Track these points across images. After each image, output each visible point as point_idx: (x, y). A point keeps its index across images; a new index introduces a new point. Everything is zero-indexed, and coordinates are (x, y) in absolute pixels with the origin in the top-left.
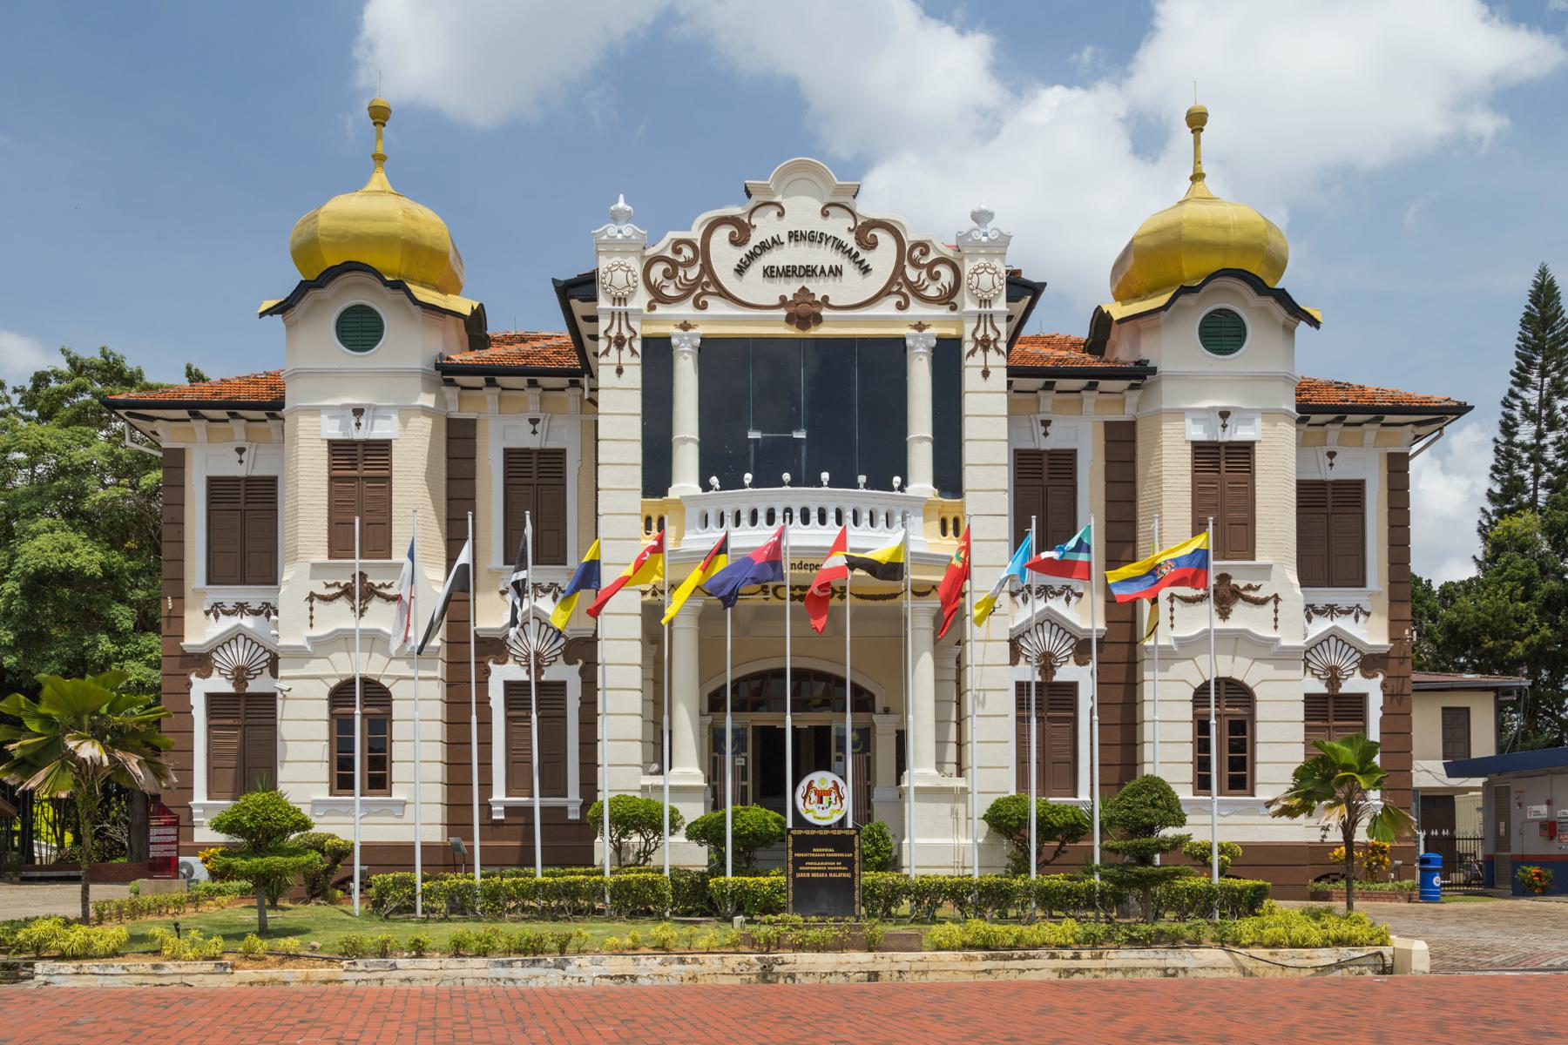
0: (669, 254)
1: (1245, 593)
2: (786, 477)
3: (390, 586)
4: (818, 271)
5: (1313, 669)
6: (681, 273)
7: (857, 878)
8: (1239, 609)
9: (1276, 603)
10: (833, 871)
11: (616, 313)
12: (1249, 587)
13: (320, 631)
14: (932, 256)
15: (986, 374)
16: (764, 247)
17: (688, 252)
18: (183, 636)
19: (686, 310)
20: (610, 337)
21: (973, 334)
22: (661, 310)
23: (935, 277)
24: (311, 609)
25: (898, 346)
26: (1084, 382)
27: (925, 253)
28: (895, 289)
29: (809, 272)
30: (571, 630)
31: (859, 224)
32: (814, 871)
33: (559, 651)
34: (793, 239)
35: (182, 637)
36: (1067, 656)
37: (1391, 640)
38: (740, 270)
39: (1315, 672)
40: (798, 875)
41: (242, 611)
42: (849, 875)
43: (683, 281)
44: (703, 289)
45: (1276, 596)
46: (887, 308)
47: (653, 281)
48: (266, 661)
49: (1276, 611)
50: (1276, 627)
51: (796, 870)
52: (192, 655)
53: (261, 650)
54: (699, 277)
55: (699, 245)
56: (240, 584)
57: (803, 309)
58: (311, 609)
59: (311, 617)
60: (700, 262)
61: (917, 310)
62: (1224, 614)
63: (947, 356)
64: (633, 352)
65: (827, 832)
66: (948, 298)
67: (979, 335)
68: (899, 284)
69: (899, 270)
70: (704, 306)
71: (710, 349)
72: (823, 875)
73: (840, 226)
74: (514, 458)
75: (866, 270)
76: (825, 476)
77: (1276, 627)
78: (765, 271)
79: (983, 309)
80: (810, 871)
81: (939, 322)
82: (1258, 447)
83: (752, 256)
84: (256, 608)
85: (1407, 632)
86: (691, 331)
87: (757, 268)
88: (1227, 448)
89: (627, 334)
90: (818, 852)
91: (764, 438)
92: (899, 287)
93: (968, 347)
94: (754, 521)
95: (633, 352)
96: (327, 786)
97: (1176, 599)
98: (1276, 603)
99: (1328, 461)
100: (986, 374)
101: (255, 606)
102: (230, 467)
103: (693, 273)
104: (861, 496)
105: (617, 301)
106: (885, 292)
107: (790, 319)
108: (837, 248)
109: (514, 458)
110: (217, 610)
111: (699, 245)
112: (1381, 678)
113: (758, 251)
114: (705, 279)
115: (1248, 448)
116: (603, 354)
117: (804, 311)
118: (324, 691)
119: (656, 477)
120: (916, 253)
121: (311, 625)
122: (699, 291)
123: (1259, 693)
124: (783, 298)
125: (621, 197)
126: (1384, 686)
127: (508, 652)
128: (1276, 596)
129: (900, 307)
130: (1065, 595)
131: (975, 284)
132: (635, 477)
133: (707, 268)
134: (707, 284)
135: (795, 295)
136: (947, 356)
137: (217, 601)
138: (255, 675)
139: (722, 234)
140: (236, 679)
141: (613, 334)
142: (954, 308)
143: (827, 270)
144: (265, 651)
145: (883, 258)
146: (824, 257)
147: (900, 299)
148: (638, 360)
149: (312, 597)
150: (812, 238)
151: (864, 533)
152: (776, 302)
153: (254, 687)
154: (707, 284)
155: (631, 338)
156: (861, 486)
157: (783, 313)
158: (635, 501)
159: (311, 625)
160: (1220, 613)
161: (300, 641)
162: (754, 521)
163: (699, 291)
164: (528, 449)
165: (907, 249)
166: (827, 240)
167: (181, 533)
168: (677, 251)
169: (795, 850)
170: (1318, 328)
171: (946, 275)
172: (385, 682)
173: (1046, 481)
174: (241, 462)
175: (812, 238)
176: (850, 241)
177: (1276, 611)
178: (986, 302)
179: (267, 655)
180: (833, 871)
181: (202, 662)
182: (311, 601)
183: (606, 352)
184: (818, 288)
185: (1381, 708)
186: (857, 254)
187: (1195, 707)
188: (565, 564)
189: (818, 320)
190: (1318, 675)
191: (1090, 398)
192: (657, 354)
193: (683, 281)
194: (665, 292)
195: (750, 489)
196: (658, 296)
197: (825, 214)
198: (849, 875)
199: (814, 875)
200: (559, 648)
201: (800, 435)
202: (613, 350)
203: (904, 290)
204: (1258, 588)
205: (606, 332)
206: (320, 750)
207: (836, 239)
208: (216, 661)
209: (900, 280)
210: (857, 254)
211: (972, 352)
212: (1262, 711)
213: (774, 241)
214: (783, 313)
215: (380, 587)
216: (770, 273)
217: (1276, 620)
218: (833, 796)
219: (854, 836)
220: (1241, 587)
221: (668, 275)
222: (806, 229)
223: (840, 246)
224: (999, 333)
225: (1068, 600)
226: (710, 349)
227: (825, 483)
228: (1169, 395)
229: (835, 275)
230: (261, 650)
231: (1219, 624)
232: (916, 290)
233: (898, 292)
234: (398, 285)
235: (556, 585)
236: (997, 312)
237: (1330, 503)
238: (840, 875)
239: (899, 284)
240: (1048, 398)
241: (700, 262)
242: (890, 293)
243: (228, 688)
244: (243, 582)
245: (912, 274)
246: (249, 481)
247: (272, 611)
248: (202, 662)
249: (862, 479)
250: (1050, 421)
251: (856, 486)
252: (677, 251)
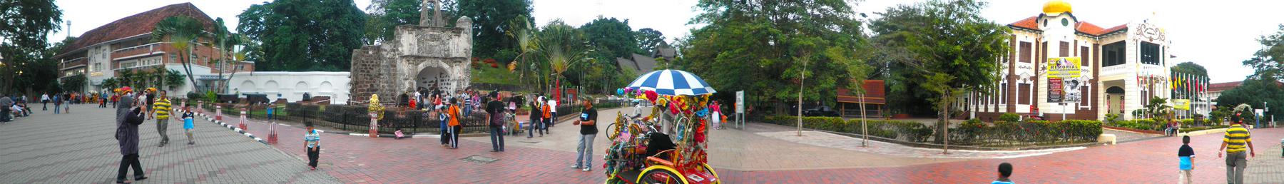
25: (1159, 45)
61: (1162, 42)
74: (1082, 47)
102: (1024, 40)
109: (1082, 47)
181: (1018, 77)
184: (1153, 36)
243: (1023, 82)
248: (1018, 77)
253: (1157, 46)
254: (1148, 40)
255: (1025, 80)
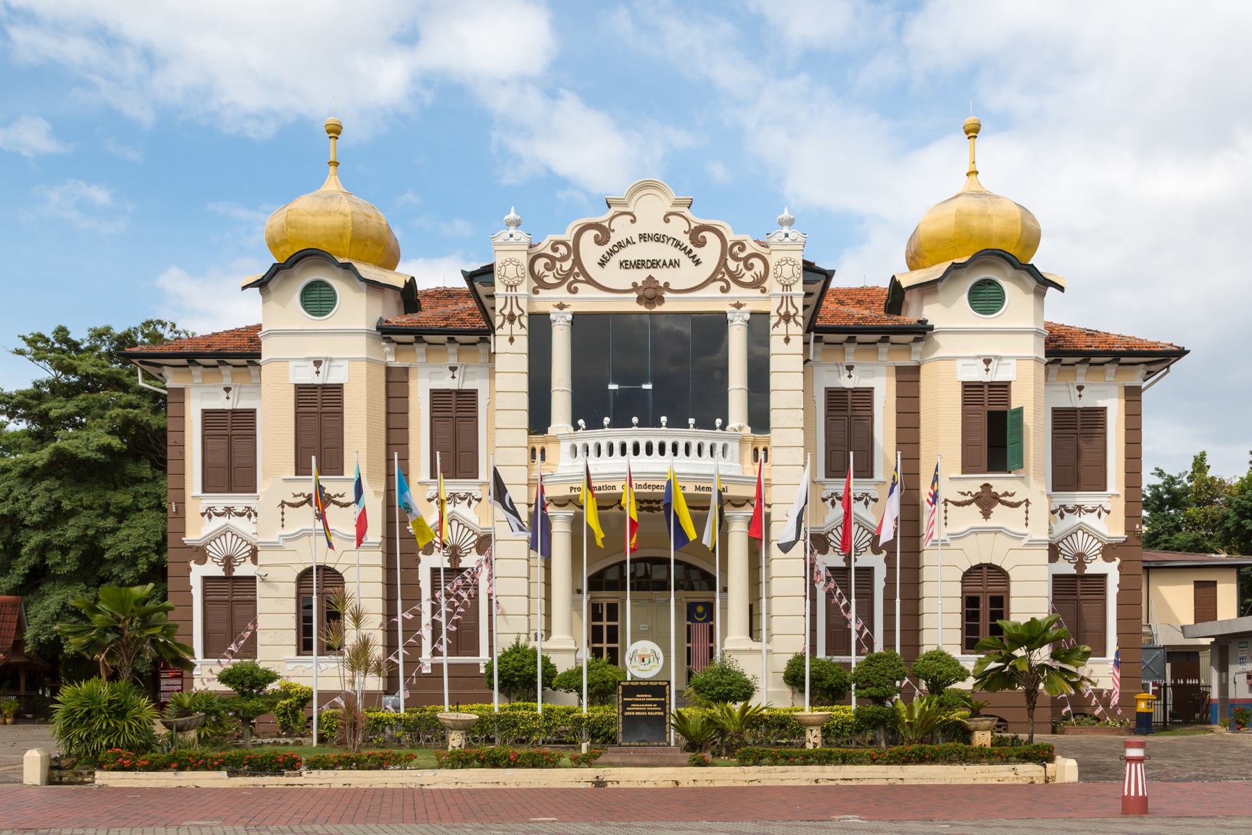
0: (549, 251)
1: (1003, 498)
2: (635, 420)
3: (342, 496)
4: (661, 264)
5: (1064, 555)
6: (558, 265)
7: (621, 712)
8: (998, 509)
9: (1027, 506)
10: (651, 711)
11: (509, 297)
12: (1006, 494)
13: (289, 530)
14: (748, 251)
15: (787, 340)
16: (620, 245)
17: (563, 250)
18: (184, 533)
19: (561, 293)
20: (504, 315)
21: (778, 311)
22: (543, 293)
23: (749, 267)
24: (283, 513)
26: (878, 337)
27: (743, 249)
28: (720, 276)
29: (654, 264)
30: (482, 529)
31: (692, 227)
32: (636, 710)
33: (473, 545)
34: (642, 240)
35: (183, 533)
36: (866, 547)
37: (1127, 532)
38: (602, 264)
39: (1066, 557)
40: (626, 714)
41: (230, 513)
42: (662, 714)
43: (560, 272)
44: (574, 278)
45: (1027, 501)
46: (714, 290)
47: (536, 272)
48: (248, 551)
49: (1027, 512)
50: (1027, 525)
51: (624, 710)
52: (191, 547)
53: (245, 543)
54: (572, 269)
55: (571, 244)
56: (228, 492)
57: (650, 293)
58: (283, 513)
59: (283, 520)
60: (572, 257)
61: (736, 291)
62: (986, 514)
63: (758, 326)
64: (522, 326)
65: (646, 683)
66: (758, 284)
67: (782, 311)
68: (723, 273)
69: (723, 263)
70: (575, 291)
71: (580, 322)
72: (643, 713)
73: (678, 229)
74: (437, 396)
75: (697, 263)
76: (664, 419)
77: (1027, 525)
78: (621, 264)
79: (785, 292)
80: (635, 711)
81: (754, 301)
82: (1012, 384)
83: (612, 253)
84: (241, 511)
85: (1137, 526)
86: (565, 310)
87: (616, 260)
88: (990, 386)
89: (517, 312)
90: (640, 697)
91: (620, 389)
92: (723, 275)
93: (773, 320)
94: (611, 453)
95: (522, 326)
96: (294, 649)
97: (948, 503)
98: (1027, 506)
99: (1078, 393)
100: (787, 340)
101: (240, 510)
103: (567, 265)
104: (690, 435)
105: (509, 288)
106: (712, 279)
107: (639, 300)
108: (676, 246)
109: (437, 396)
110: (209, 513)
111: (571, 245)
112: (1118, 560)
113: (616, 249)
114: (576, 270)
115: (1006, 386)
116: (499, 328)
117: (651, 293)
118: (292, 575)
119: (539, 420)
120: (736, 249)
121: (283, 526)
122: (572, 279)
123: (1013, 575)
124: (635, 284)
125: (513, 208)
126: (1120, 567)
127: (434, 545)
128: (1027, 501)
129: (723, 290)
130: (864, 500)
131: (779, 273)
132: (523, 419)
133: (578, 262)
134: (578, 275)
135: (643, 282)
136: (758, 326)
137: (210, 506)
138: (240, 562)
139: (590, 235)
140: (225, 565)
141: (506, 312)
142: (764, 291)
143: (668, 263)
144: (247, 544)
145: (710, 253)
146: (665, 252)
147: (724, 284)
148: (525, 332)
149: (283, 504)
150: (658, 238)
151: (693, 462)
152: (631, 287)
153: (239, 571)
154: (578, 275)
155: (520, 315)
156: (691, 426)
157: (635, 295)
158: (522, 437)
159: (283, 526)
160: (983, 514)
161: (276, 540)
162: (611, 453)
163: (572, 279)
164: (448, 390)
165: (729, 246)
166: (668, 240)
167: (182, 453)
168: (555, 249)
169: (624, 696)
170: (1063, 292)
171: (758, 266)
172: (339, 569)
173: (850, 413)
174: (228, 398)
175: (658, 238)
176: (685, 239)
177: (1027, 512)
178: (787, 286)
179: (249, 547)
180: (651, 711)
181: (200, 554)
182: (283, 507)
183: (501, 326)
184: (661, 275)
185: (1118, 586)
186: (691, 251)
187: (963, 586)
188: (477, 478)
189: (661, 300)
190: (1069, 560)
191: (883, 348)
192: (539, 326)
193: (560, 272)
194: (546, 280)
195: (608, 429)
196: (541, 284)
197: (667, 220)
198: (662, 714)
199: (637, 713)
200: (473, 542)
201: (648, 386)
202: (507, 324)
203: (726, 277)
204: (1013, 494)
205: (501, 311)
206: (290, 622)
207: (674, 239)
208: (210, 551)
209: (723, 270)
210: (691, 251)
211: (777, 325)
212: (1015, 589)
213: (628, 242)
214: (635, 295)
215: (335, 496)
216: (625, 265)
217: (1027, 519)
218: (652, 658)
219: (665, 686)
220: (1000, 494)
221: (548, 268)
222: (652, 231)
223: (678, 244)
224: (797, 309)
225: (866, 503)
226: (580, 322)
227: (664, 424)
228: (945, 345)
229: (674, 267)
230: (245, 543)
231: (983, 523)
232: (735, 277)
233: (722, 279)
234: (347, 267)
235: (470, 494)
236: (795, 294)
237: (1079, 426)
238: (656, 713)
239: (723, 273)
240: (850, 348)
241: (572, 257)
242: (715, 280)
243: (219, 572)
244: (230, 491)
245: (732, 265)
246: (234, 412)
247: (252, 513)
248: (200, 554)
249: (691, 421)
250: (853, 366)
251: (687, 426)
252: (555, 249)
253: (714, 326)
254: (630, 304)
255: (229, 562)
